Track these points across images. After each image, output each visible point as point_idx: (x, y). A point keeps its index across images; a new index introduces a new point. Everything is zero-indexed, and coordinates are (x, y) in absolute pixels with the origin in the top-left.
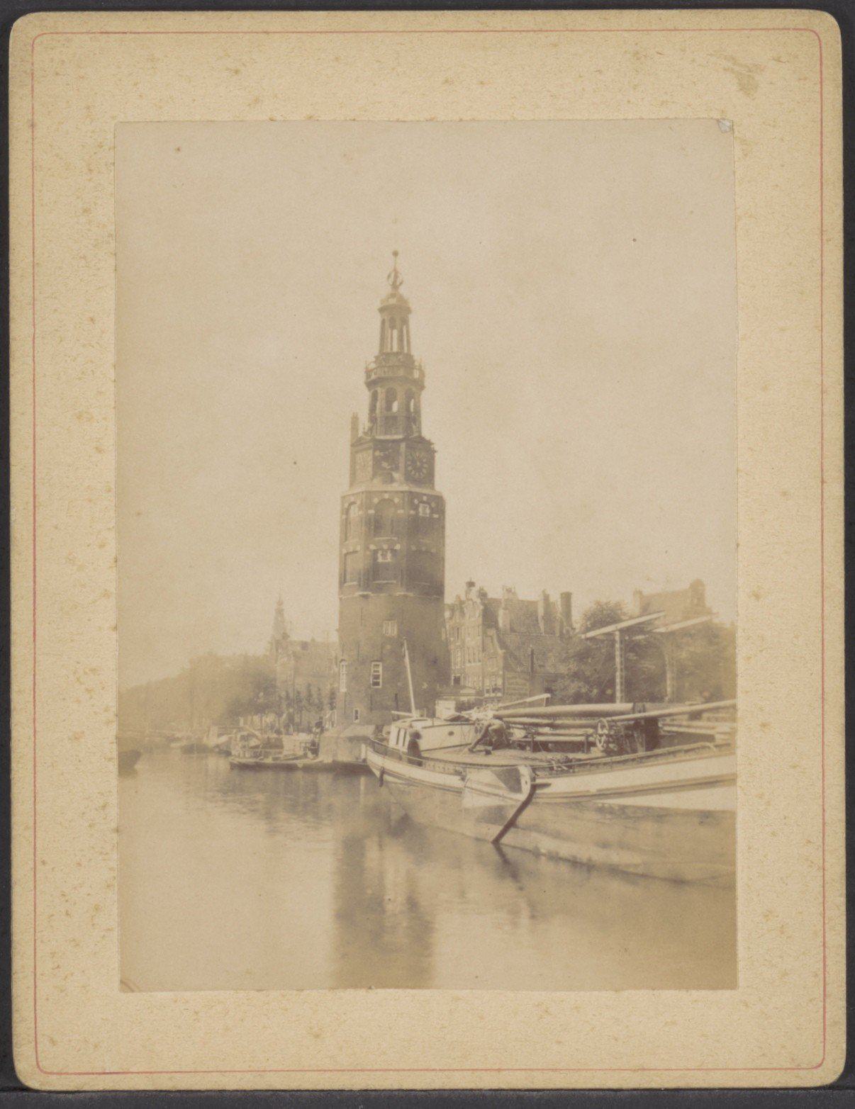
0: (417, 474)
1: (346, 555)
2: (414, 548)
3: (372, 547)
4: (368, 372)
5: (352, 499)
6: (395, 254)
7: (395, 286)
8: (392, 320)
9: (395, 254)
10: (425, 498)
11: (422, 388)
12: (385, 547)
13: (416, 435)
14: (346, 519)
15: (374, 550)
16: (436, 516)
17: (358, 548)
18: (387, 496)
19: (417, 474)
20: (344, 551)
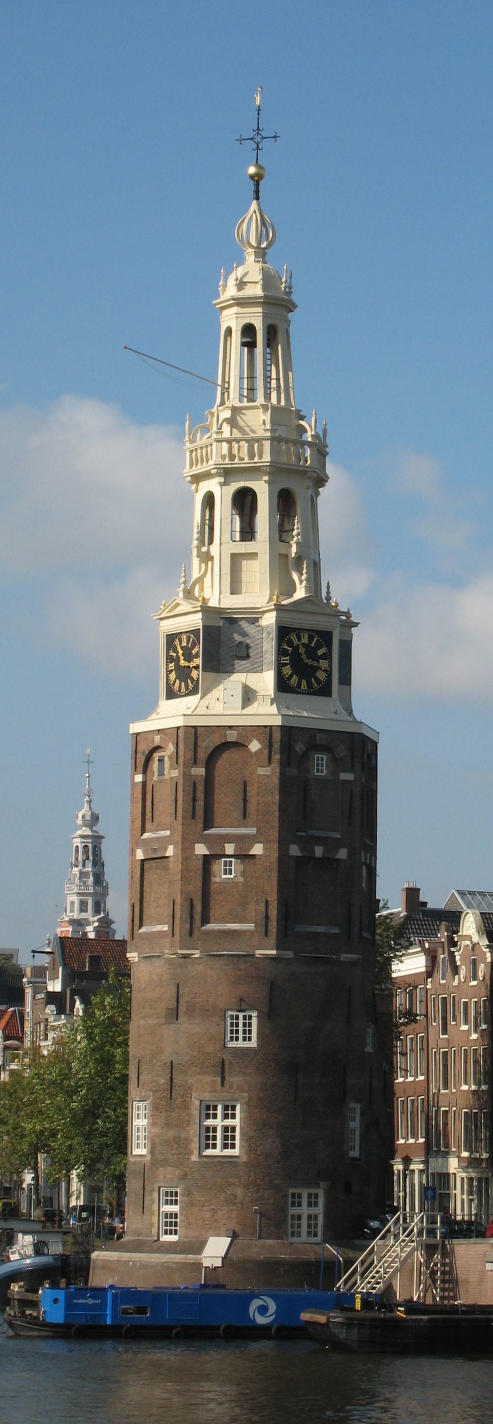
0: (304, 682)
1: (142, 861)
2: (294, 850)
3: (201, 849)
5: (157, 740)
8: (248, 330)
10: (320, 739)
11: (321, 481)
12: (230, 849)
13: (300, 593)
14: (144, 783)
15: (205, 855)
17: (170, 851)
18: (232, 736)
19: (304, 682)
20: (140, 855)
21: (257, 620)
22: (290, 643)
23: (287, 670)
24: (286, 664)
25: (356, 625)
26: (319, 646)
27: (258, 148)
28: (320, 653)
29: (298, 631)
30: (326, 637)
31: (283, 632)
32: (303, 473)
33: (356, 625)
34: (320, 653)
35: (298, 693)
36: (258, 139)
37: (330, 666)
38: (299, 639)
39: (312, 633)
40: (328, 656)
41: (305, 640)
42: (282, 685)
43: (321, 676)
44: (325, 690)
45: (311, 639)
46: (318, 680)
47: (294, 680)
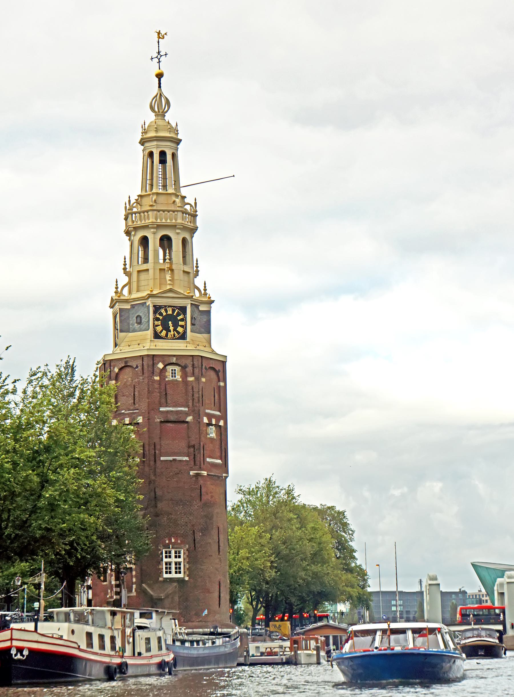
6: (160, 76)
9: (160, 76)
21: (145, 303)
22: (161, 314)
23: (159, 329)
24: (159, 325)
25: (213, 301)
26: (178, 314)
27: (159, 62)
28: (179, 318)
29: (165, 307)
30: (183, 310)
31: (157, 309)
32: (174, 227)
33: (213, 301)
34: (179, 318)
35: (166, 339)
36: (159, 57)
37: (186, 324)
38: (166, 311)
39: (174, 308)
40: (184, 320)
41: (170, 312)
42: (157, 336)
43: (180, 329)
44: (183, 337)
45: (173, 311)
46: (178, 333)
47: (164, 332)
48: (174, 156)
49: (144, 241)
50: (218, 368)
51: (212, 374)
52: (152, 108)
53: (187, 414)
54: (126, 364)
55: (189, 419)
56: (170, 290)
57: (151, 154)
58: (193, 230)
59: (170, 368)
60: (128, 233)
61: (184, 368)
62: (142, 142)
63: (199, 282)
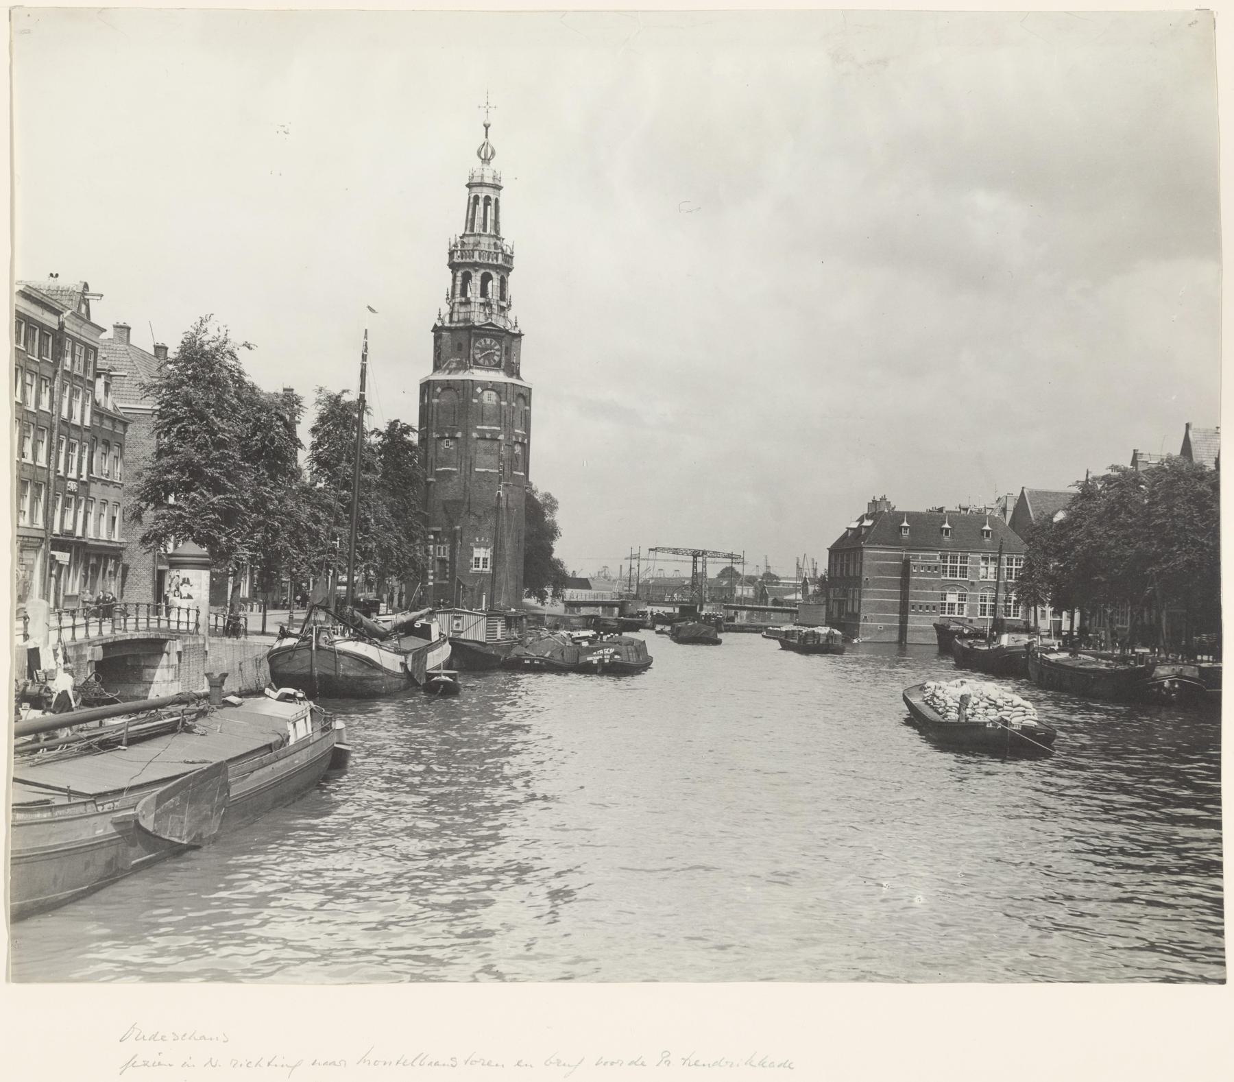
2: (475, 435)
4: (451, 254)
6: (487, 127)
7: (486, 160)
8: (476, 198)
9: (487, 127)
16: (504, 403)
48: (497, 200)
49: (467, 278)
50: (524, 396)
51: (521, 401)
52: (479, 153)
53: (499, 433)
54: (448, 386)
55: (501, 437)
56: (491, 324)
57: (476, 198)
58: (510, 270)
59: (486, 393)
60: (453, 266)
61: (498, 393)
62: (469, 186)
63: (511, 314)
